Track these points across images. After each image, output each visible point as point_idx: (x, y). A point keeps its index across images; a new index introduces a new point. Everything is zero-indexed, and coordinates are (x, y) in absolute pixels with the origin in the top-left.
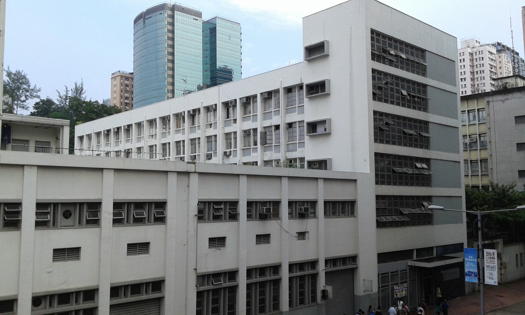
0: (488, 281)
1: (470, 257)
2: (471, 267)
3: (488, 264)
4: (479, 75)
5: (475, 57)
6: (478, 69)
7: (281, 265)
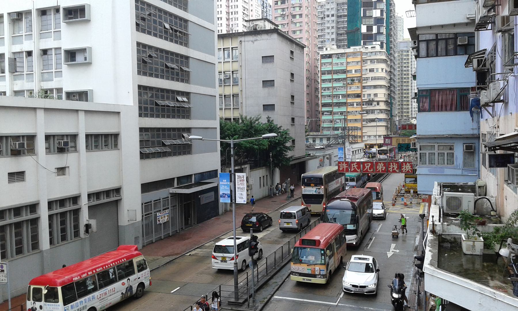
0: (239, 201)
3: (239, 186)
6: (233, 10)
7: (80, 196)
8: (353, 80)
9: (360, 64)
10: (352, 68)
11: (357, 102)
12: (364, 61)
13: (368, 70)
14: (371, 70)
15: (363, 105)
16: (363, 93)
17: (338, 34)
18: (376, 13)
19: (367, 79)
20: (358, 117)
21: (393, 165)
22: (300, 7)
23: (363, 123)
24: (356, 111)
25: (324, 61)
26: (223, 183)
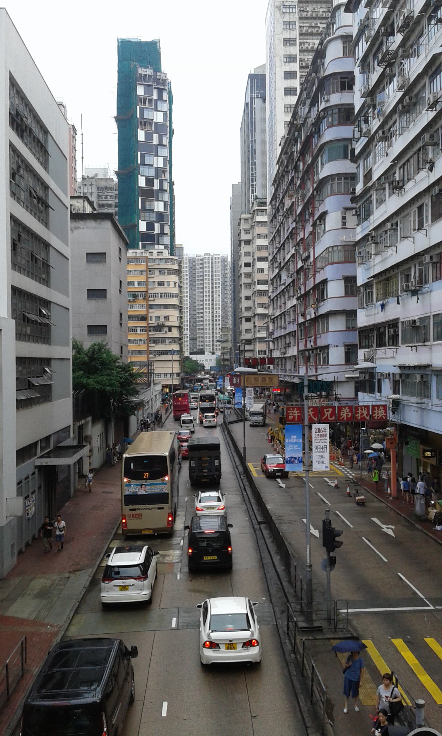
0: (317, 467)
1: (292, 437)
2: (294, 451)
3: (325, 444)
8: (135, 296)
9: (144, 273)
11: (141, 327)
12: (150, 271)
13: (156, 283)
14: (161, 284)
15: (150, 331)
16: (150, 315)
18: (159, 207)
19: (155, 295)
20: (143, 347)
21: (362, 409)
23: (150, 356)
24: (141, 340)
26: (290, 441)
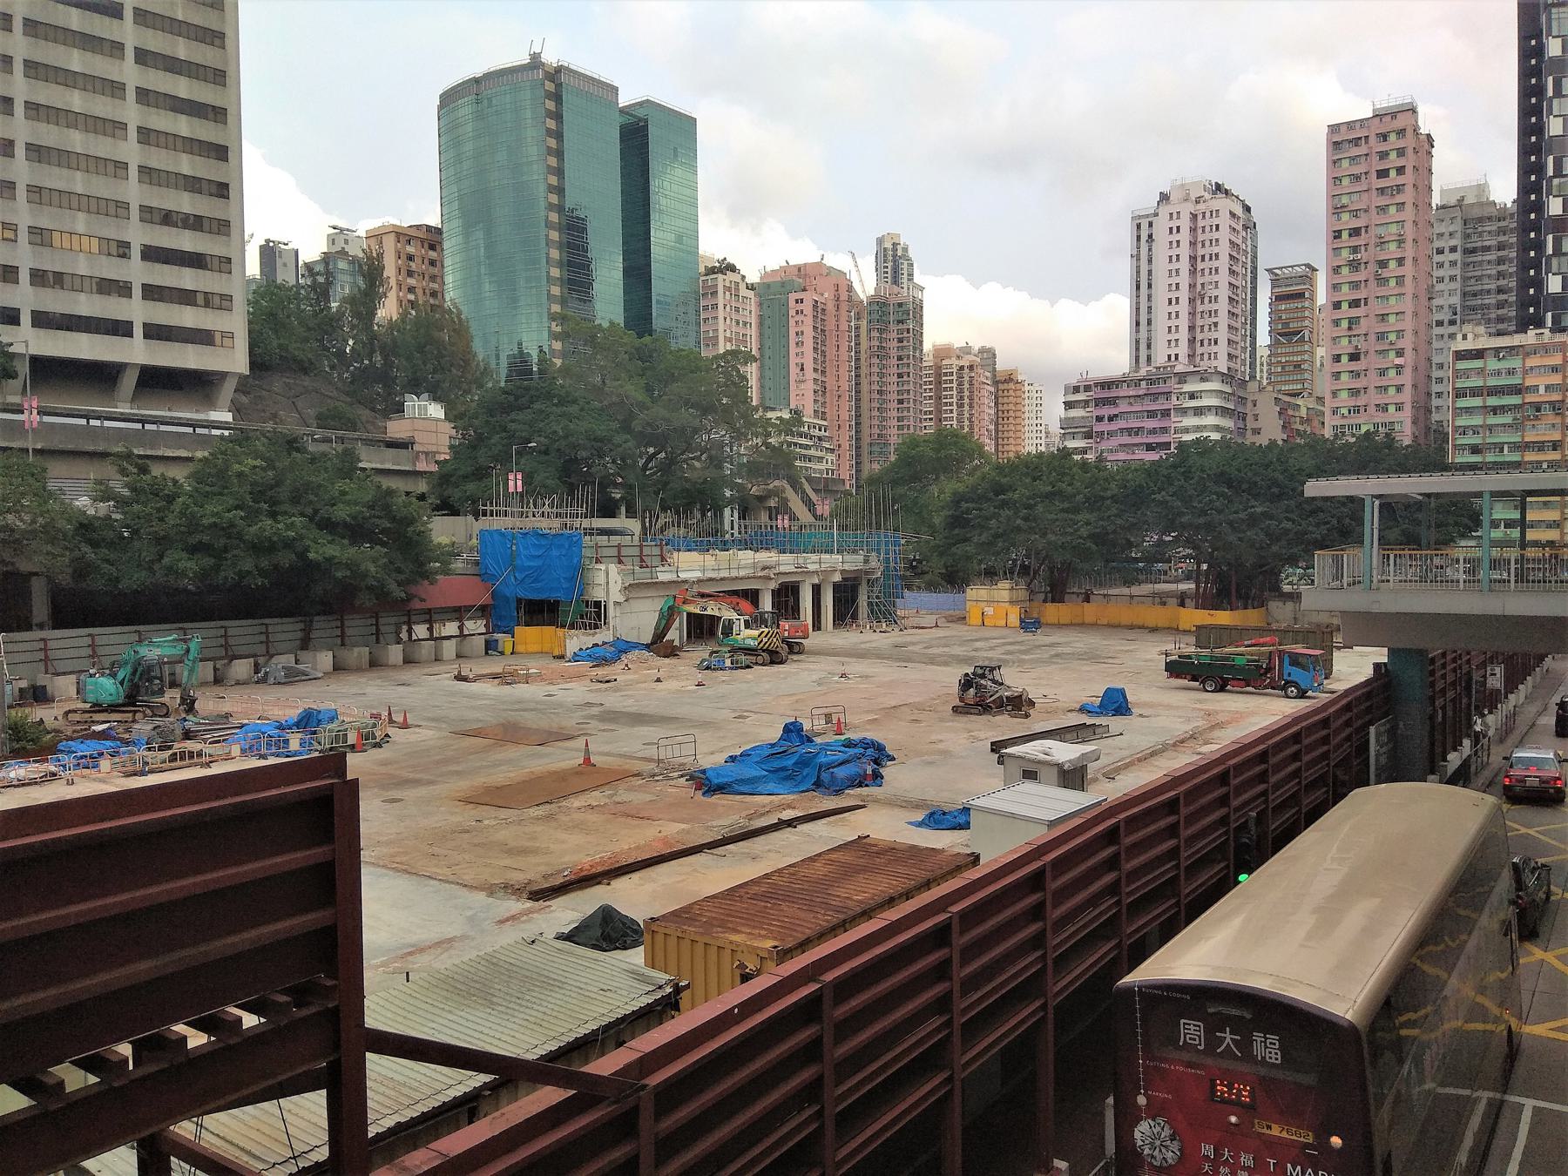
4: (1207, 265)
5: (1201, 223)
6: (1207, 251)
8: (1538, 410)
10: (1541, 381)
17: (1464, 294)
22: (1401, 242)
25: (1462, 365)
